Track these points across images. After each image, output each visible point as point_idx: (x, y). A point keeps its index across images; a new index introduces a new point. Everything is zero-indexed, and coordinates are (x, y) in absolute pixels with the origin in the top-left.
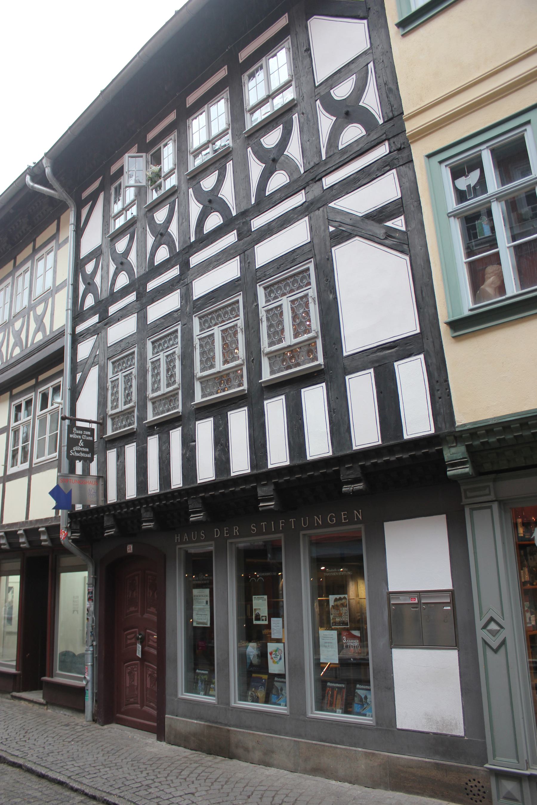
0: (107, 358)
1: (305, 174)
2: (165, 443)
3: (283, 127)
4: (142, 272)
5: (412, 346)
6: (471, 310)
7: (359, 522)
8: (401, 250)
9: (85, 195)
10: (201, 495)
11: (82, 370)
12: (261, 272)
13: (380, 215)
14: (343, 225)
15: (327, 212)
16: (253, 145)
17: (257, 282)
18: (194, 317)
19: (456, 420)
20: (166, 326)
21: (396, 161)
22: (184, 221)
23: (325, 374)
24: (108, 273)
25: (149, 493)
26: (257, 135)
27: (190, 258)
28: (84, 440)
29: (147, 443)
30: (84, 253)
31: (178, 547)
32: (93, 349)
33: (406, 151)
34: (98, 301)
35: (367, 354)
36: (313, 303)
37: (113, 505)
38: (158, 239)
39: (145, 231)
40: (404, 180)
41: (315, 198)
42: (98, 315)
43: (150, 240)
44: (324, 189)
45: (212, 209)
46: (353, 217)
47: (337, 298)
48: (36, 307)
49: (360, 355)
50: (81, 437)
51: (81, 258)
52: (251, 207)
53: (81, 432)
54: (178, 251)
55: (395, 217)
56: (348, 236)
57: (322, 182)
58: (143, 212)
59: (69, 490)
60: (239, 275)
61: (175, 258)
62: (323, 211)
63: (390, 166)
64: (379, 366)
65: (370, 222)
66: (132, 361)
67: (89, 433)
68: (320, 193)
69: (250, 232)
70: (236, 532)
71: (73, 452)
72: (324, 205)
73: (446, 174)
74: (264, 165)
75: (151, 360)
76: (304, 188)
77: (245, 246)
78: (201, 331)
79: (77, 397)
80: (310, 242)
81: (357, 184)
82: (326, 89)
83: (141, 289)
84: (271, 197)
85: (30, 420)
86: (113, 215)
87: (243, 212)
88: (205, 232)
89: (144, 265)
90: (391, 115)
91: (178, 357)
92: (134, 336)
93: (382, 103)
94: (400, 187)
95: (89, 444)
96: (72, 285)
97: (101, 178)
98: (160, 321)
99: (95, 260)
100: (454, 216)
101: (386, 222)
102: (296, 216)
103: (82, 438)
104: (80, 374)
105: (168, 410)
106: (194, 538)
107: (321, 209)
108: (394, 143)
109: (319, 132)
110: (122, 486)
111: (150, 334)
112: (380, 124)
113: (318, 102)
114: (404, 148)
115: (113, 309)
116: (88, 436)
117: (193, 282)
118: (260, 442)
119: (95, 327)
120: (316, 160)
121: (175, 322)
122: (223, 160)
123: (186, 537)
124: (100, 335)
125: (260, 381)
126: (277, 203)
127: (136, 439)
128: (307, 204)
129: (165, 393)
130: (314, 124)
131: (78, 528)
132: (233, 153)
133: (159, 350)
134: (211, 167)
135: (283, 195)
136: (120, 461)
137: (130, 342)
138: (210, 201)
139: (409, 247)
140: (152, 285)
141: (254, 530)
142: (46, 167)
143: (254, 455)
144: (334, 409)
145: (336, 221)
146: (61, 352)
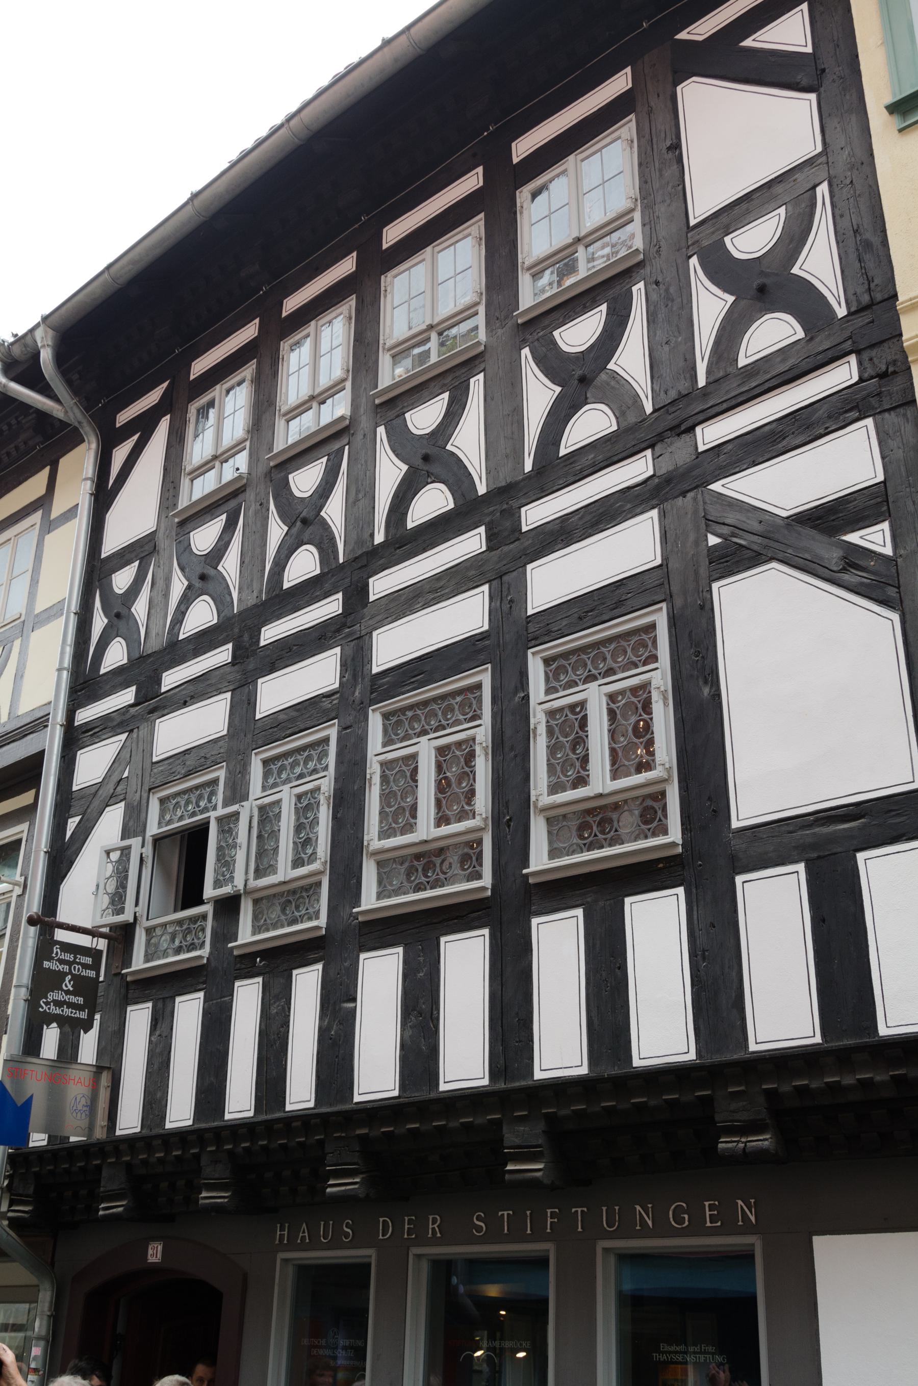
1: (656, 414)
2: (277, 998)
3: (608, 308)
4: (251, 601)
5: (902, 819)
7: (748, 1229)
8: (881, 599)
9: (124, 417)
10: (358, 1132)
11: (82, 810)
12: (538, 623)
13: (832, 518)
14: (741, 533)
15: (705, 503)
16: (536, 343)
17: (530, 645)
18: (370, 711)
20: (302, 727)
21: (873, 401)
22: (360, 496)
23: (684, 868)
24: (166, 595)
25: (227, 1117)
26: (546, 321)
27: (371, 580)
28: (75, 978)
29: (232, 995)
30: (111, 544)
31: (281, 1255)
32: (116, 765)
33: (899, 380)
34: (137, 656)
35: (791, 829)
36: (661, 703)
37: (131, 1141)
38: (295, 530)
39: (264, 510)
40: (893, 444)
41: (676, 469)
42: (134, 688)
43: (276, 531)
44: (700, 450)
45: (429, 474)
46: (767, 517)
47: (719, 695)
49: (772, 828)
50: (70, 969)
51: (103, 556)
52: (523, 480)
53: (69, 957)
54: (341, 561)
55: (867, 523)
56: (750, 559)
57: (695, 435)
58: (261, 469)
59: (28, 1096)
60: (486, 627)
61: (333, 576)
62: (695, 499)
63: (860, 411)
64: (819, 857)
65: (807, 531)
66: (210, 801)
67: (89, 960)
68: (688, 460)
69: (517, 534)
70: (433, 1229)
71: (47, 1003)
72: (696, 487)
74: (558, 389)
75: (259, 802)
76: (652, 446)
77: (505, 562)
78: (384, 745)
79: (64, 872)
80: (660, 566)
81: (780, 446)
82: (713, 233)
83: (246, 637)
84: (571, 460)
86: (189, 468)
88: (410, 525)
89: (256, 585)
90: (866, 299)
91: (328, 799)
92: (221, 743)
93: (846, 273)
94: (883, 458)
95: (85, 987)
96: (75, 614)
97: (165, 385)
98: (286, 714)
99: (137, 563)
101: (846, 533)
102: (629, 506)
103: (70, 973)
104: (78, 819)
105: (294, 921)
107: (690, 495)
108: (871, 359)
109: (692, 325)
110: (159, 1095)
111: (260, 742)
112: (839, 317)
113: (694, 261)
114: (895, 373)
115: (171, 679)
116: (85, 966)
117: (375, 634)
118: (517, 1014)
119: (124, 714)
120: (683, 386)
121: (325, 719)
122: (463, 371)
123: (304, 1233)
124: (135, 735)
125: (525, 871)
126: (585, 473)
127: (204, 983)
128: (657, 480)
129: (287, 879)
130: (682, 308)
131: (31, 1190)
132: (487, 356)
133: (278, 780)
134: (433, 384)
135: (600, 457)
136: (158, 1033)
137: (208, 756)
138: (426, 458)
139: (899, 592)
140: (271, 633)
141: (479, 1229)
142: (43, 346)
143: (500, 1043)
144: (704, 951)
145: (724, 524)
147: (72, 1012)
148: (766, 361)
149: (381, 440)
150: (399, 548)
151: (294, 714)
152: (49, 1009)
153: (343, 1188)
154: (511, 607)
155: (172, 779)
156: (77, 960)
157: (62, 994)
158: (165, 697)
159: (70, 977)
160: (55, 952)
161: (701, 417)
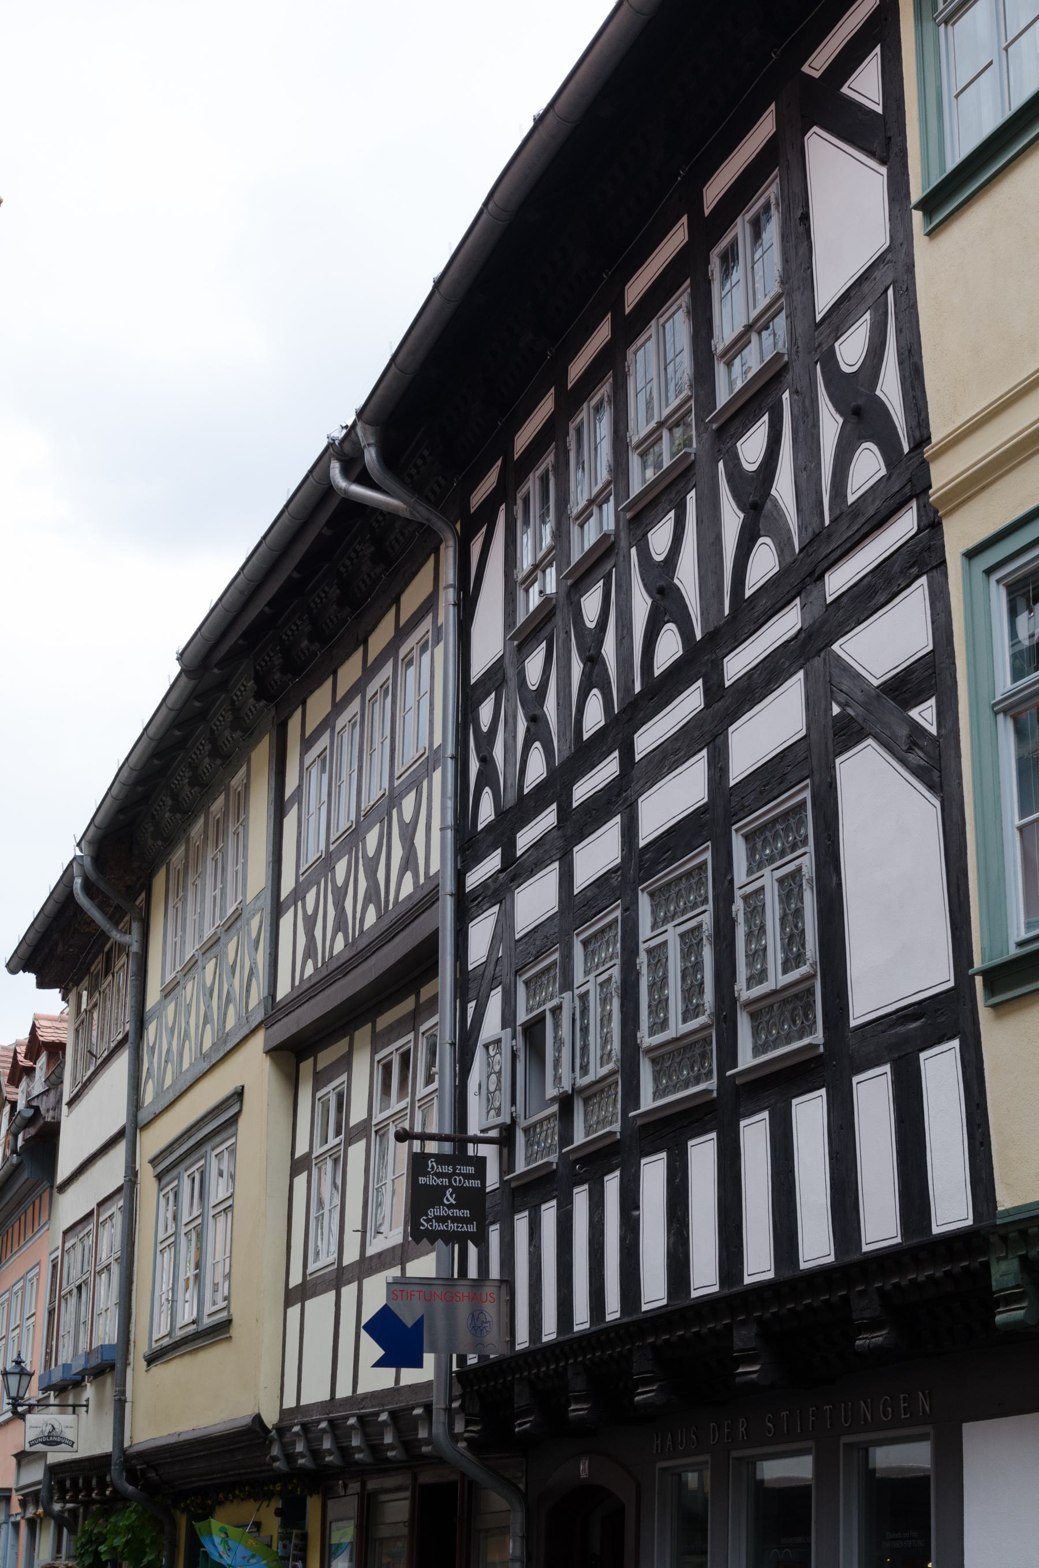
0: (514, 971)
4: (566, 754)
6: (1021, 944)
17: (733, 822)
19: (998, 1199)
20: (601, 906)
24: (515, 737)
28: (456, 1190)
29: (572, 1203)
32: (494, 942)
47: (841, 884)
48: (402, 798)
50: (450, 1182)
53: (448, 1169)
67: (471, 1170)
68: (821, 613)
70: (742, 1431)
71: (428, 1221)
73: (999, 599)
76: (798, 594)
78: (653, 929)
85: (406, 1108)
97: (499, 463)
100: (1005, 711)
103: (451, 1185)
106: (714, 1440)
109: (820, 450)
116: (468, 1177)
127: (556, 1190)
146: (430, 946)
147: (458, 1227)
148: (864, 501)
150: (652, 699)
152: (431, 1226)
153: (645, 1396)
154: (721, 776)
156: (457, 1171)
157: (443, 1209)
158: (519, 863)
159: (451, 1190)
160: (430, 1167)
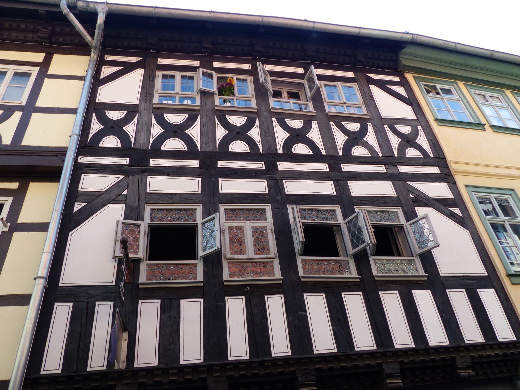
0: (144, 203)
1: (383, 157)
9: (108, 58)
10: (317, 367)
22: (267, 135)
54: (261, 152)
55: (453, 207)
64: (467, 289)
68: (397, 173)
76: (385, 165)
87: (331, 155)
90: (438, 156)
99: (125, 112)
104: (84, 204)
113: (386, 126)
114: (448, 175)
124: (131, 177)
128: (388, 174)
140: (222, 164)
149: (275, 122)
151: (244, 196)
155: (163, 203)
158: (153, 169)
161: (399, 164)
